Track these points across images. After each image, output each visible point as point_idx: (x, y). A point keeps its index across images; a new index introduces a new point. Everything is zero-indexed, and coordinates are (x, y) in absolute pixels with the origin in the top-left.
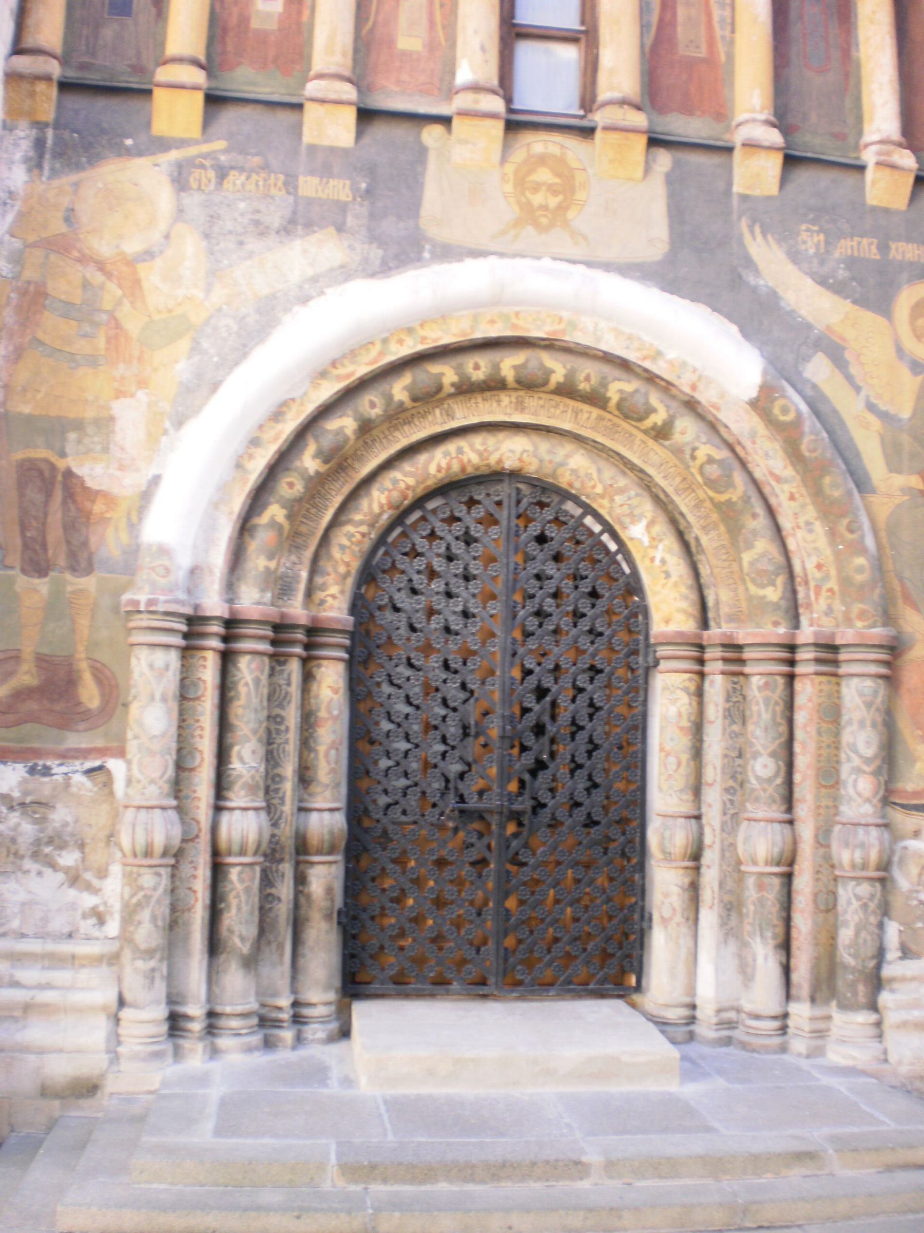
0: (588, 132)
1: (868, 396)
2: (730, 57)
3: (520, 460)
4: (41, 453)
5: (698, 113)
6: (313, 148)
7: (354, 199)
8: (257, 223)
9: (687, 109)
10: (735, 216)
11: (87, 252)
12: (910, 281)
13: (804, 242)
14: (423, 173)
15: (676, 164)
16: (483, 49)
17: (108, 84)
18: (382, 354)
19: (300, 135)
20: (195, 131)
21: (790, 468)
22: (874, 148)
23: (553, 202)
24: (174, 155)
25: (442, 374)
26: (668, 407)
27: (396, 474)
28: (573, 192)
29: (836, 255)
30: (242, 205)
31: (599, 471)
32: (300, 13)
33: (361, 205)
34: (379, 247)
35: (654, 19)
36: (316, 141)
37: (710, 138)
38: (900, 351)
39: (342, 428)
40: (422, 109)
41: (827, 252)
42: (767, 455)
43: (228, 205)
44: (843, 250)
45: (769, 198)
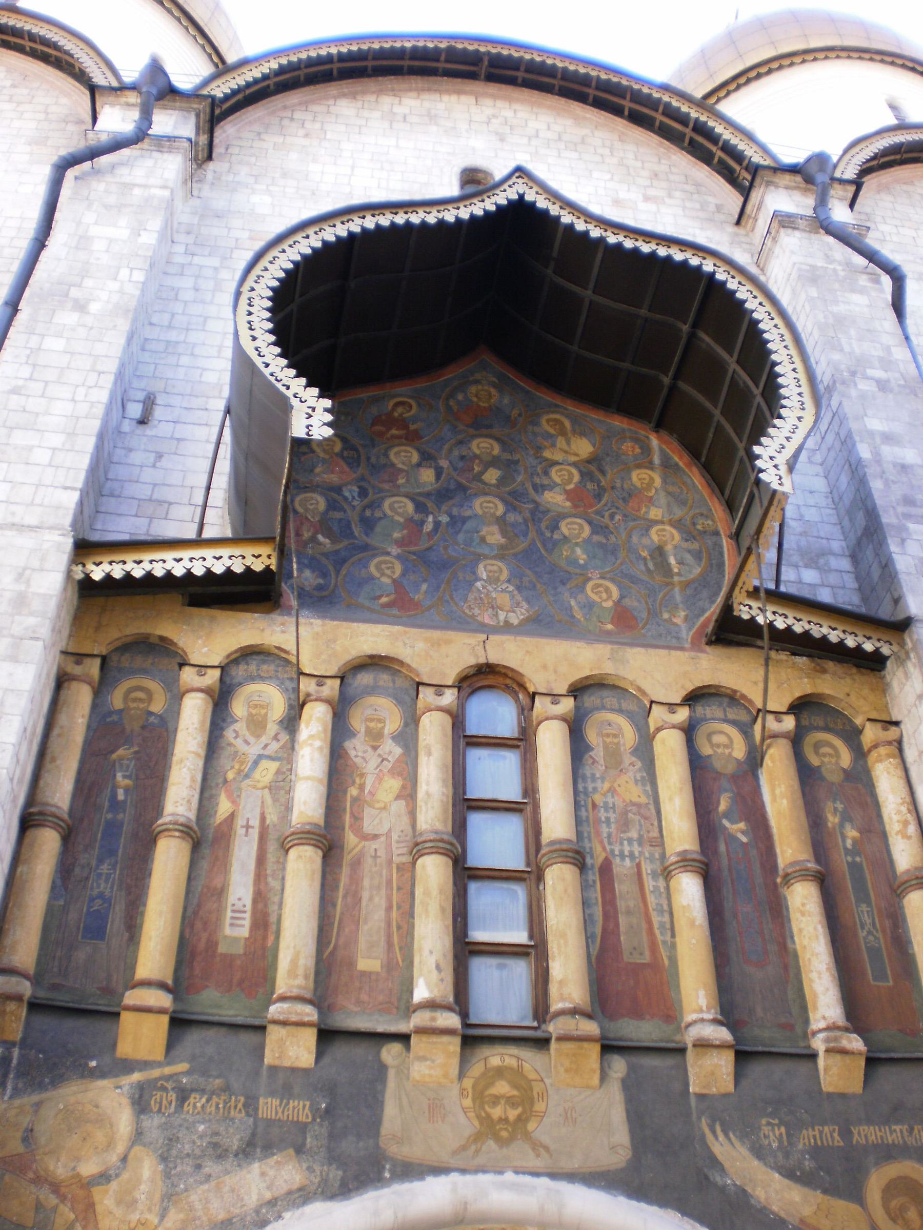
0: (542, 1043)
2: (673, 960)
5: (648, 1017)
6: (273, 1069)
7: (314, 1119)
8: (215, 1145)
9: (637, 1013)
10: (694, 1116)
11: (42, 1173)
12: (877, 1164)
14: (383, 1092)
15: (631, 1068)
16: (438, 967)
17: (76, 1006)
19: (262, 1057)
20: (158, 1054)
22: (821, 1036)
23: (513, 1114)
24: (136, 1077)
29: (800, 1146)
30: (201, 1128)
32: (265, 938)
33: (321, 1126)
34: (338, 1169)
35: (598, 930)
36: (277, 1063)
37: (661, 1041)
40: (380, 1029)
41: (790, 1143)
43: (188, 1128)
44: (806, 1140)
45: (726, 1095)
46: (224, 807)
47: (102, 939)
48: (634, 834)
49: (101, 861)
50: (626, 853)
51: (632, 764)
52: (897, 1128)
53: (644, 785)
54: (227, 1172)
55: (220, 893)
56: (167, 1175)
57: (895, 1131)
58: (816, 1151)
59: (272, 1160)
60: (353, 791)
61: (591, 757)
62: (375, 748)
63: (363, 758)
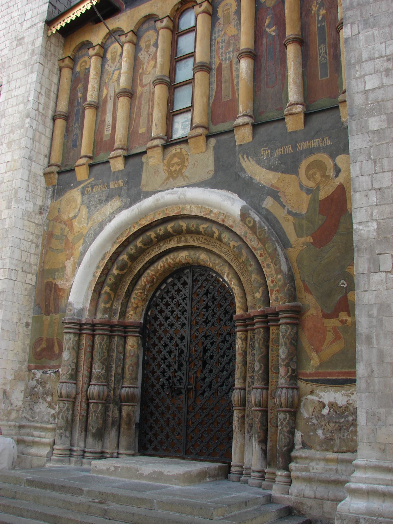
1: (288, 208)
3: (185, 259)
4: (51, 279)
6: (114, 172)
13: (262, 155)
15: (217, 142)
18: (129, 232)
20: (87, 178)
21: (260, 244)
23: (178, 168)
24: (82, 185)
25: (151, 235)
26: (218, 230)
27: (148, 271)
28: (184, 163)
29: (275, 156)
30: (97, 196)
31: (210, 258)
38: (301, 186)
39: (123, 258)
41: (271, 156)
42: (251, 241)
44: (278, 154)
46: (105, 92)
47: (76, 147)
48: (231, 49)
49: (75, 123)
50: (227, 58)
51: (234, 19)
52: (317, 140)
53: (237, 26)
54: (102, 207)
55: (103, 121)
56: (89, 212)
57: (316, 142)
58: (281, 157)
59: (113, 201)
60: (140, 71)
61: (219, 23)
62: (147, 52)
63: (144, 57)
